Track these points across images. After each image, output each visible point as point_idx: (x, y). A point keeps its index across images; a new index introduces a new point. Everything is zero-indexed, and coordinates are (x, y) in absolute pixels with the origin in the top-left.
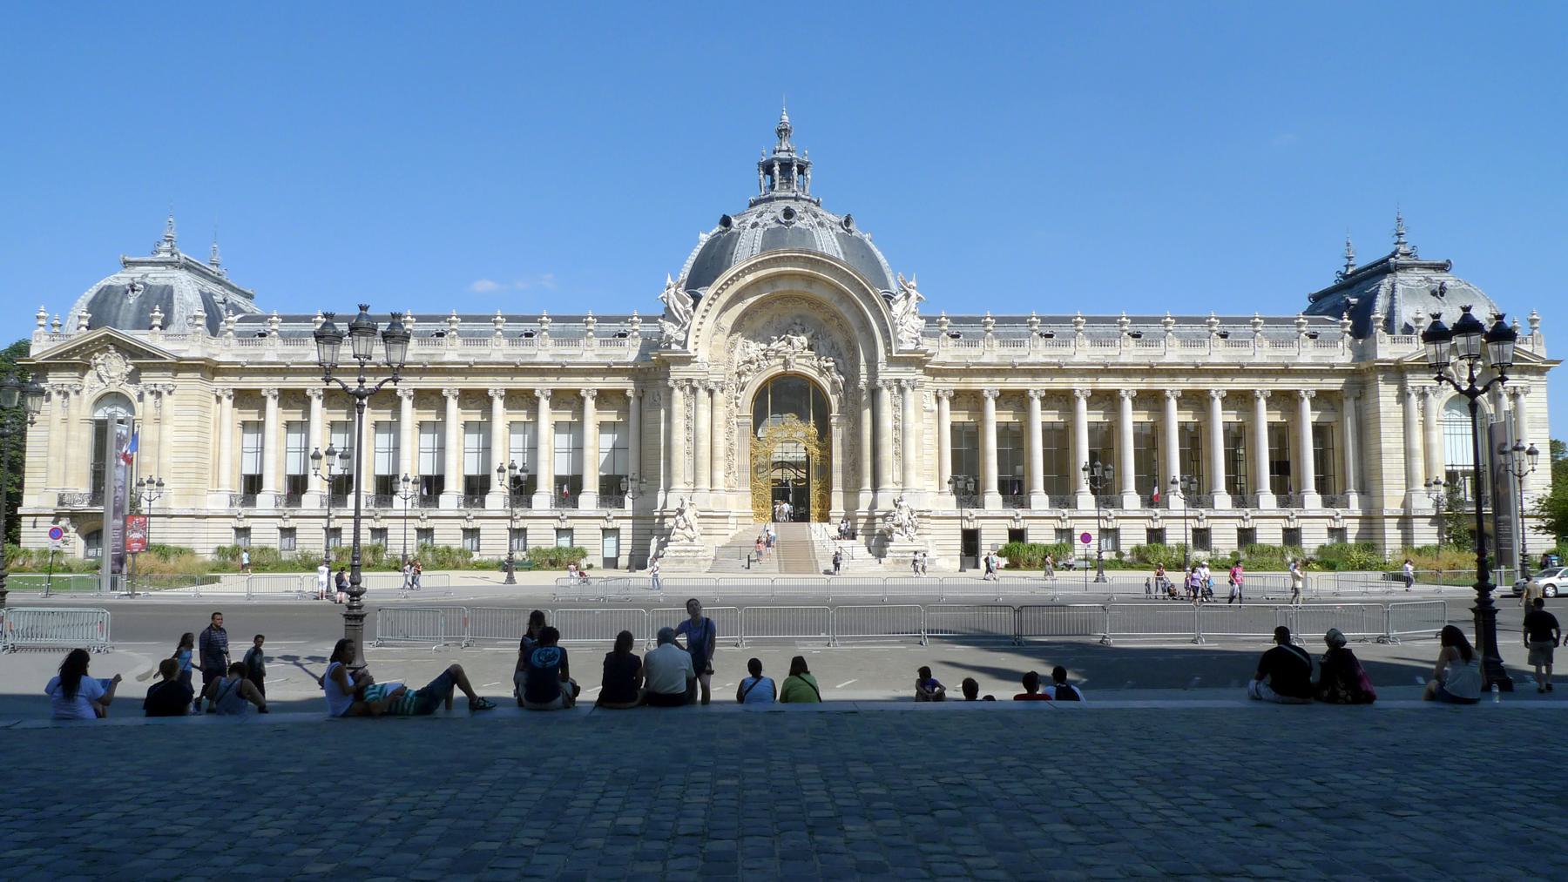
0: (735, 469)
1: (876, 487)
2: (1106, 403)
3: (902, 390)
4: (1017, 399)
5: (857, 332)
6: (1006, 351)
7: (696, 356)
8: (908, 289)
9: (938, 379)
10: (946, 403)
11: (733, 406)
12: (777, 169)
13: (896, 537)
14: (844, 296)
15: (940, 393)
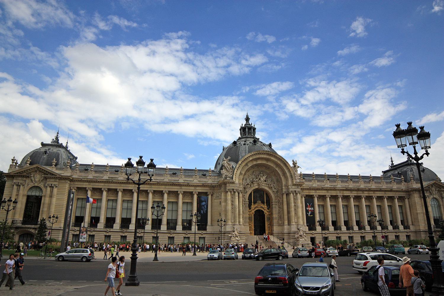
1: (289, 224)
3: (296, 194)
6: (319, 183)
11: (243, 198)
14: (278, 165)
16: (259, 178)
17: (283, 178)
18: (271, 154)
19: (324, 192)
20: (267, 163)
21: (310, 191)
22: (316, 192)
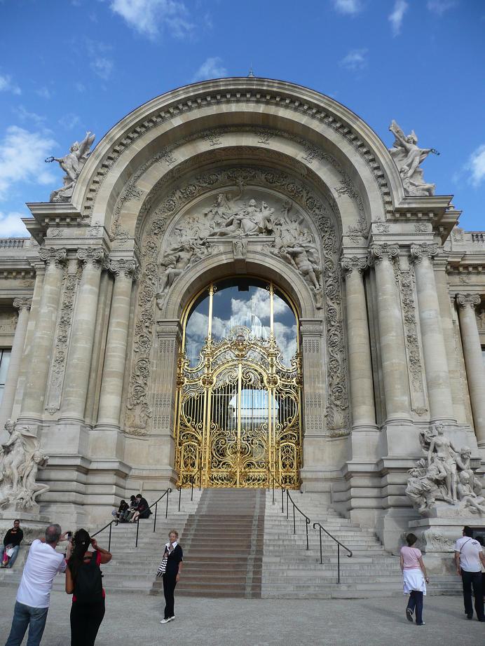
3: (413, 259)
5: (335, 195)
7: (88, 217)
13: (440, 507)
15: (461, 299)
16: (235, 222)
20: (263, 146)
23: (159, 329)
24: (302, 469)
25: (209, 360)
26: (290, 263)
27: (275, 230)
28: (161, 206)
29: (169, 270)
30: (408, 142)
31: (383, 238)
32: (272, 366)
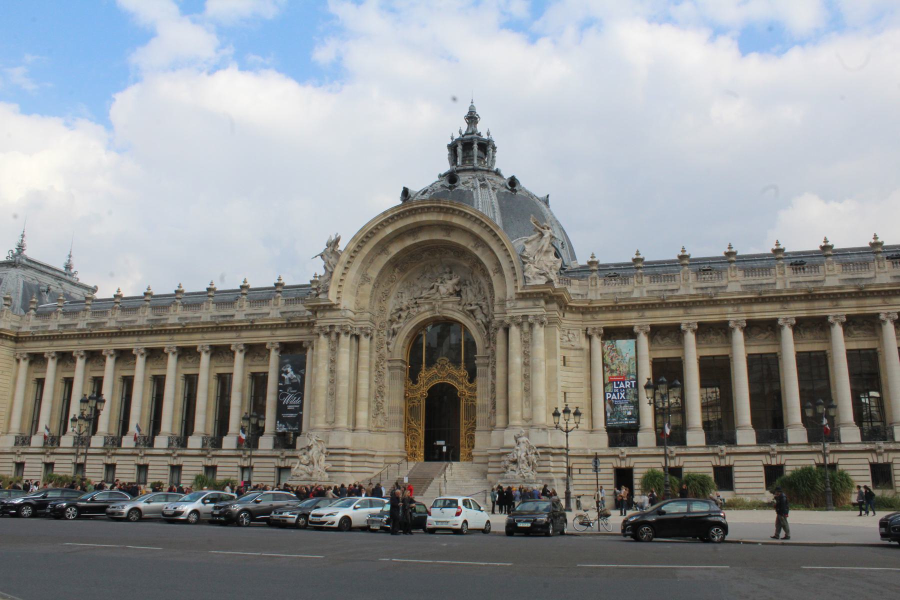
0: (385, 409)
2: (768, 334)
4: (673, 334)
5: (491, 274)
6: (655, 286)
7: (339, 304)
8: (542, 230)
9: (588, 317)
10: (597, 341)
12: (459, 150)
15: (589, 332)
16: (435, 287)
17: (495, 279)
18: (448, 209)
19: (672, 312)
20: (447, 238)
21: (619, 315)
22: (642, 317)
23: (390, 365)
24: (473, 450)
25: (423, 381)
26: (470, 316)
27: (463, 290)
28: (386, 280)
29: (395, 326)
30: (544, 229)
31: (513, 311)
32: (462, 384)
